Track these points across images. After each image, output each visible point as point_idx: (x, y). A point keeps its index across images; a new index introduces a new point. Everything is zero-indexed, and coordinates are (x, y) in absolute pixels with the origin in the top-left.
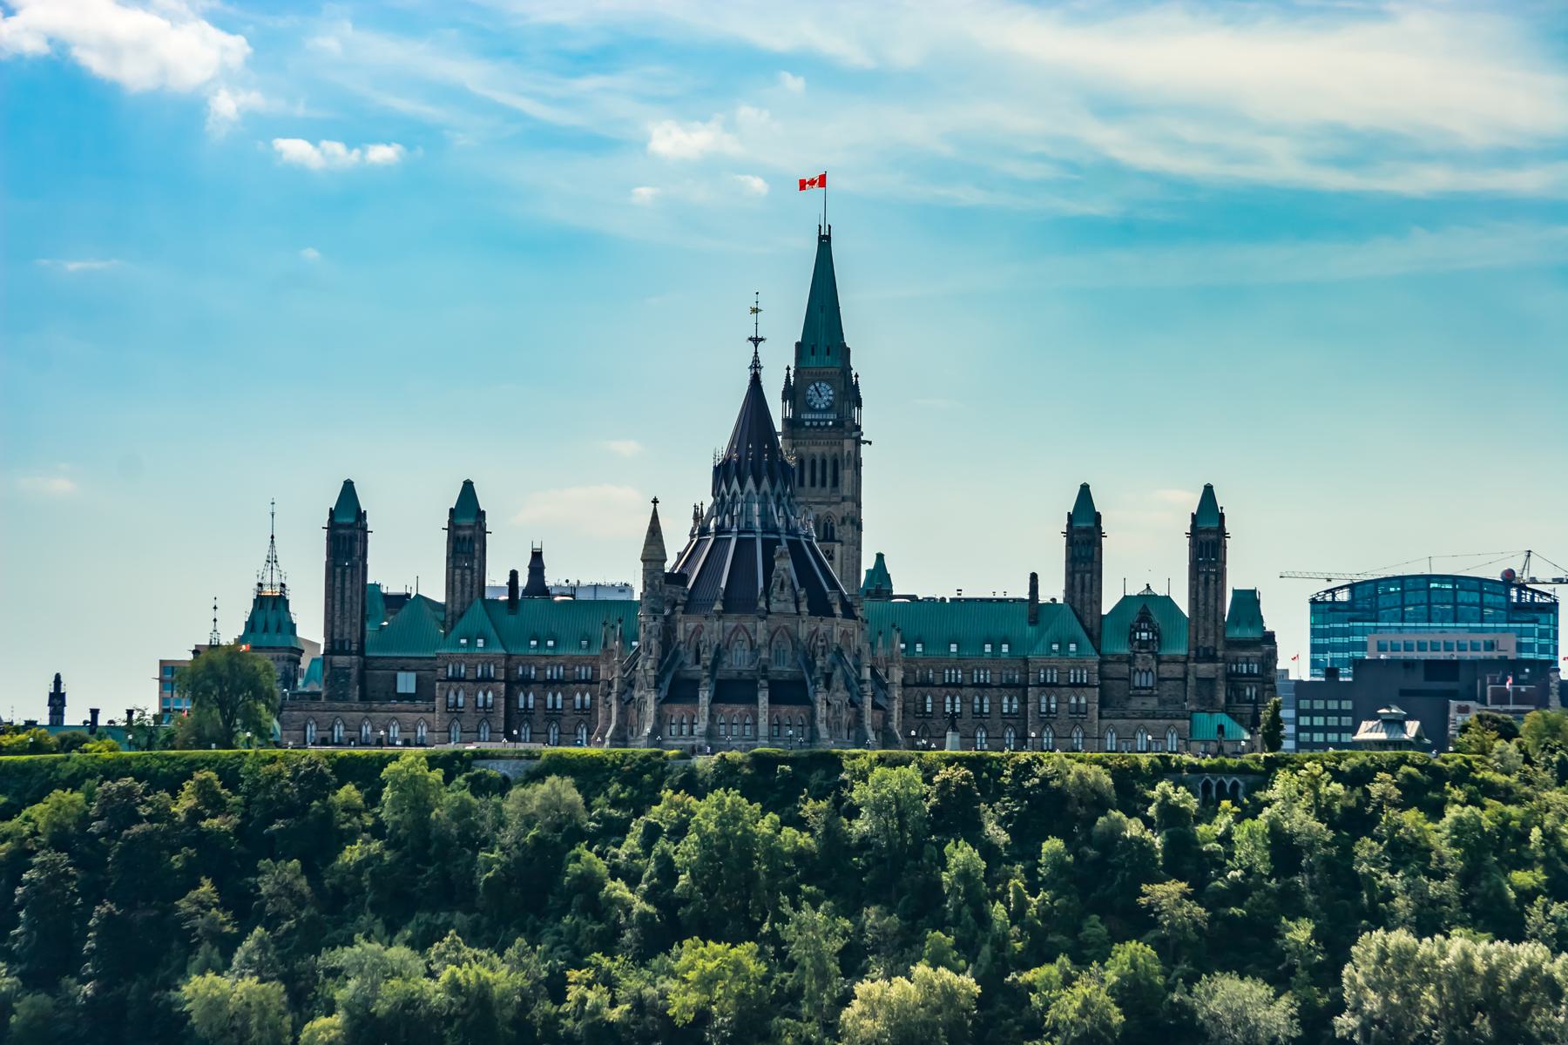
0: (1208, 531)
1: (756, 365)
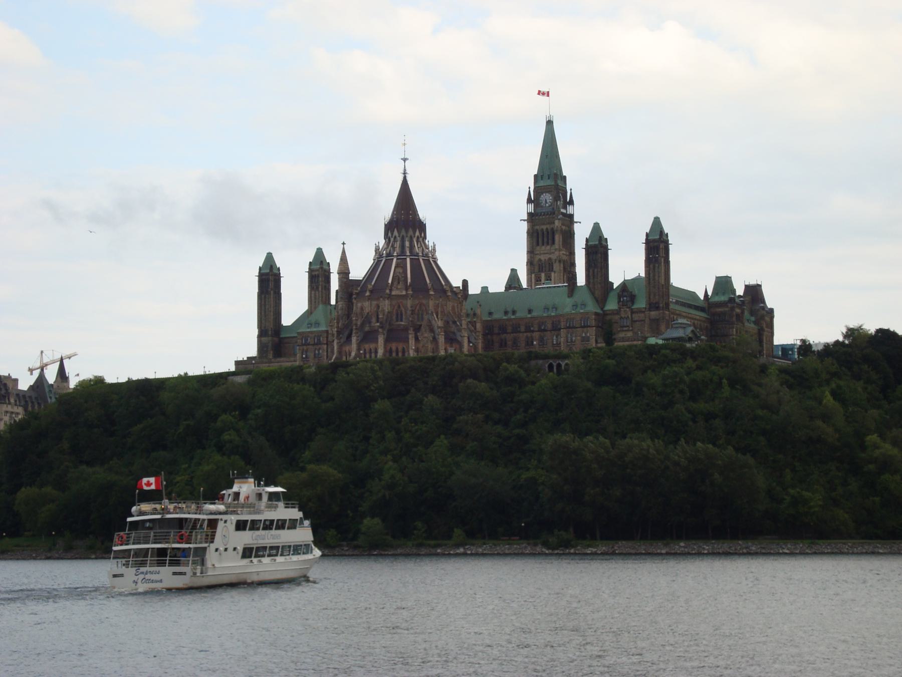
0: (654, 241)
1: (405, 173)
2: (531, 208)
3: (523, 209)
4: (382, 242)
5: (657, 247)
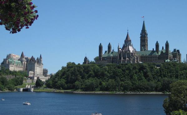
1: (128, 32)
2: (141, 36)
3: (140, 36)
4: (124, 43)
5: (167, 45)
